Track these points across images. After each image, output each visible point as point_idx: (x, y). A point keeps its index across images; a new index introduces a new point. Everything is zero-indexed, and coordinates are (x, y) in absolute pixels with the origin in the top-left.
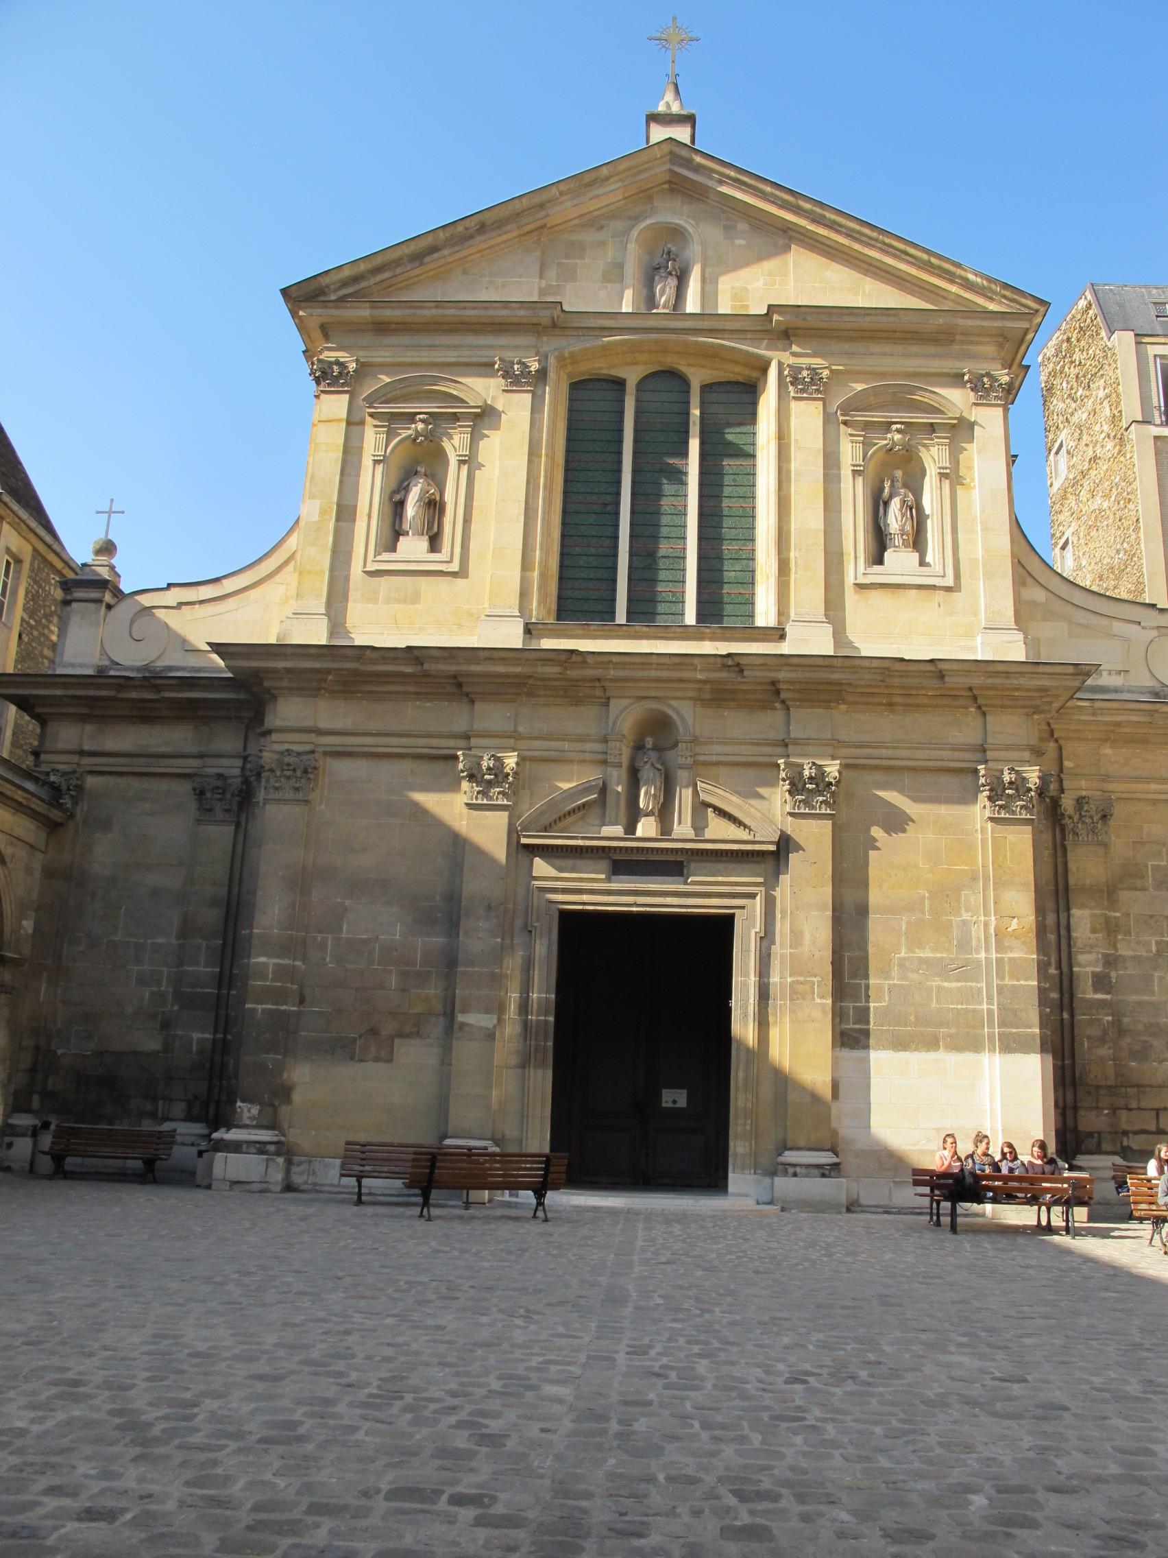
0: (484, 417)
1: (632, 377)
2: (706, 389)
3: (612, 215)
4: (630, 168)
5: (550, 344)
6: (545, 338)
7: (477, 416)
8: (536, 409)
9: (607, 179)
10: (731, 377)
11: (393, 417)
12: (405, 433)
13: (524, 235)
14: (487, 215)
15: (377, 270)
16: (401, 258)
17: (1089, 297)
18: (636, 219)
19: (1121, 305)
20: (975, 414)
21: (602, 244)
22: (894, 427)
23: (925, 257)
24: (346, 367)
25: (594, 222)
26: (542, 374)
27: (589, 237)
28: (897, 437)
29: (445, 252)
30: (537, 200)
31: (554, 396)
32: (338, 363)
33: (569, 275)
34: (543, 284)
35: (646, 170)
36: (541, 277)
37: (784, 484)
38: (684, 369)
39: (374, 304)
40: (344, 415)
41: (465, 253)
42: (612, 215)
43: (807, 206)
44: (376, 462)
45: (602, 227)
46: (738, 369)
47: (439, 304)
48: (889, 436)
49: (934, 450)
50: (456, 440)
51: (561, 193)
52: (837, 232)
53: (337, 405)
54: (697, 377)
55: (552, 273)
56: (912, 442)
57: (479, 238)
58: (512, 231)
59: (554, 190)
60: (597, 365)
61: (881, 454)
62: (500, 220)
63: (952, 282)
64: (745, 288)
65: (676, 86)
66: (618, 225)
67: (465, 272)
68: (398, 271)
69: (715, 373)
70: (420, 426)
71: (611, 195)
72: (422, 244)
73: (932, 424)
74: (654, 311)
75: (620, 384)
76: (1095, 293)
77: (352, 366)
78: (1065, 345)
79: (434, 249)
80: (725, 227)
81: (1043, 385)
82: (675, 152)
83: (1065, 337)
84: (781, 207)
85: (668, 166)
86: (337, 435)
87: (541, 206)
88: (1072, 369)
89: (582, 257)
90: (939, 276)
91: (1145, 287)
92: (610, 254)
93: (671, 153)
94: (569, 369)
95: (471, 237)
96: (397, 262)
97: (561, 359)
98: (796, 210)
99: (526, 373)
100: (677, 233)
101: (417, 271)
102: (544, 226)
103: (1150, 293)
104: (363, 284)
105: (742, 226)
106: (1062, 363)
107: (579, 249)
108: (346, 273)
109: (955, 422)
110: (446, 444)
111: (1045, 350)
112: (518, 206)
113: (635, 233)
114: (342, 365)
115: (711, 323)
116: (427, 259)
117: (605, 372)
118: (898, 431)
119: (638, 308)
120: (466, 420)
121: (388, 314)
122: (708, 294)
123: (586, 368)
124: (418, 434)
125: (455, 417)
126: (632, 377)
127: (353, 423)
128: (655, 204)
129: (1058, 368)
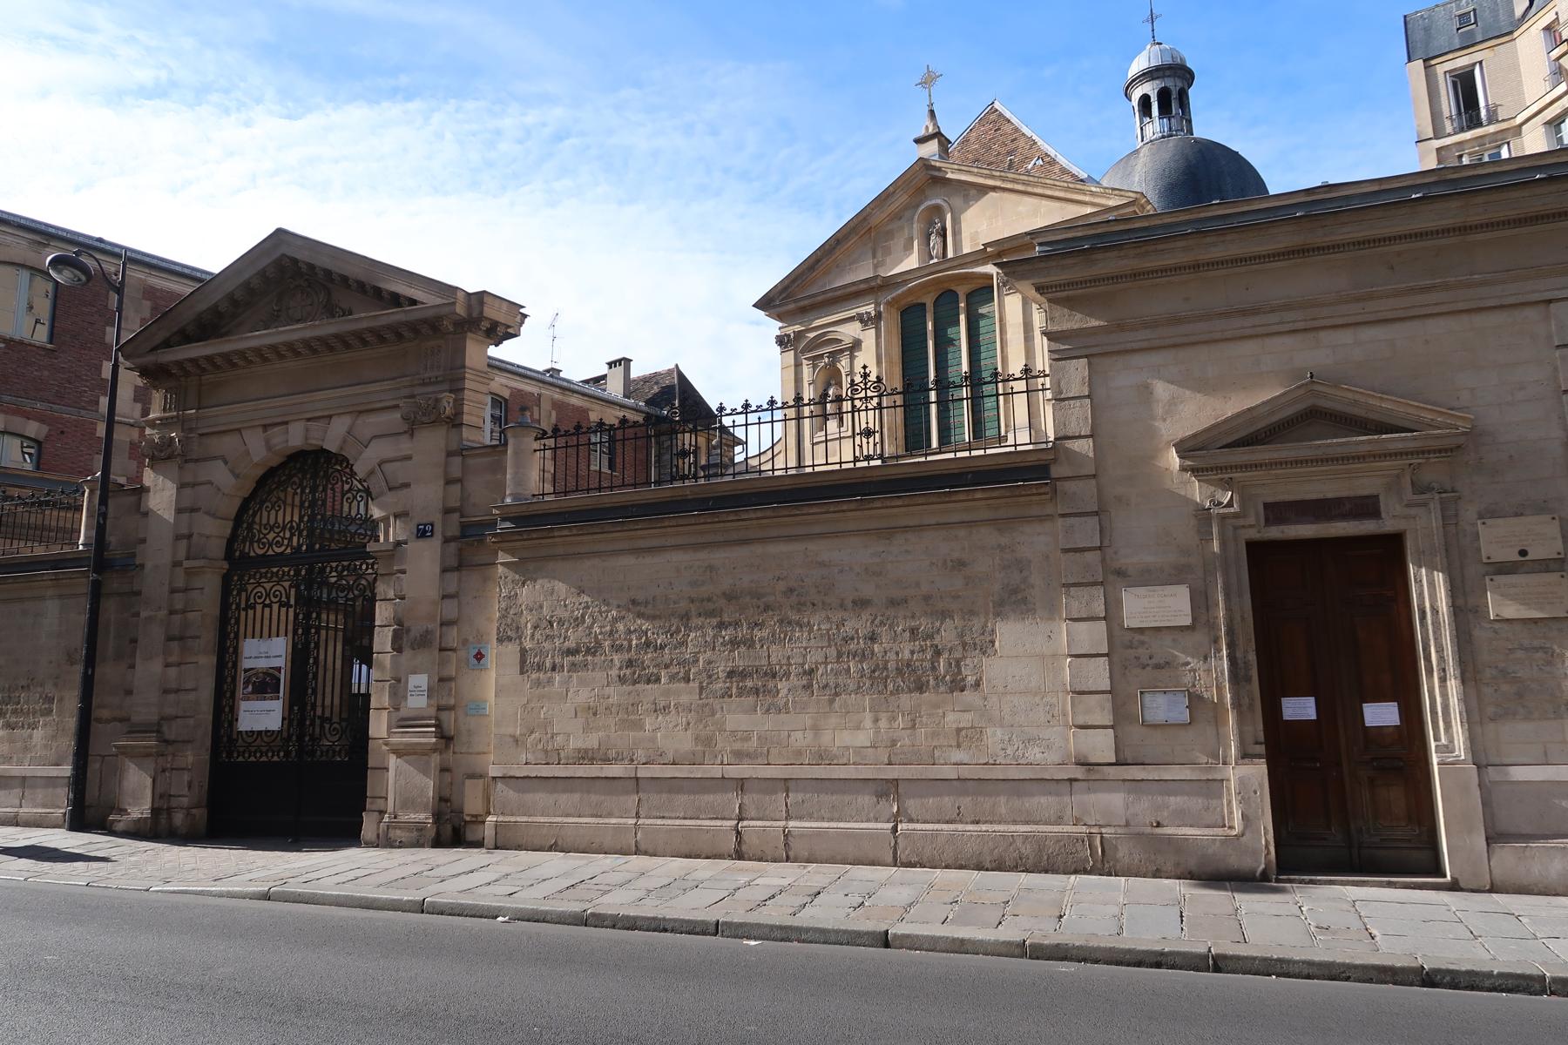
1: (929, 301)
3: (906, 207)
8: (878, 336)
10: (979, 286)
11: (814, 358)
13: (862, 236)
14: (839, 235)
15: (794, 281)
18: (918, 206)
21: (902, 228)
23: (1066, 185)
25: (897, 216)
26: (879, 316)
30: (861, 218)
31: (891, 324)
33: (888, 251)
34: (875, 261)
35: (915, 177)
36: (874, 257)
37: (1005, 348)
38: (953, 288)
39: (795, 301)
40: (793, 363)
41: (834, 257)
44: (810, 384)
45: (901, 218)
46: (981, 281)
47: (824, 293)
50: (843, 363)
51: (873, 209)
52: (1018, 183)
54: (962, 291)
55: (879, 254)
57: (839, 247)
60: (910, 299)
62: (845, 235)
63: (1085, 194)
64: (977, 232)
66: (908, 214)
67: (837, 266)
68: (804, 277)
70: (826, 360)
71: (901, 199)
72: (811, 261)
74: (931, 262)
77: (792, 335)
79: (818, 261)
84: (986, 178)
85: (924, 173)
87: (865, 219)
89: (892, 239)
90: (1077, 193)
95: (834, 248)
96: (802, 274)
97: (888, 304)
99: (870, 319)
101: (815, 274)
102: (871, 227)
104: (790, 290)
105: (973, 192)
107: (890, 235)
108: (780, 288)
110: (839, 366)
112: (852, 224)
113: (916, 217)
114: (789, 336)
116: (816, 267)
117: (915, 302)
119: (924, 262)
120: (846, 351)
121: (802, 303)
124: (826, 365)
125: (842, 351)
127: (798, 365)
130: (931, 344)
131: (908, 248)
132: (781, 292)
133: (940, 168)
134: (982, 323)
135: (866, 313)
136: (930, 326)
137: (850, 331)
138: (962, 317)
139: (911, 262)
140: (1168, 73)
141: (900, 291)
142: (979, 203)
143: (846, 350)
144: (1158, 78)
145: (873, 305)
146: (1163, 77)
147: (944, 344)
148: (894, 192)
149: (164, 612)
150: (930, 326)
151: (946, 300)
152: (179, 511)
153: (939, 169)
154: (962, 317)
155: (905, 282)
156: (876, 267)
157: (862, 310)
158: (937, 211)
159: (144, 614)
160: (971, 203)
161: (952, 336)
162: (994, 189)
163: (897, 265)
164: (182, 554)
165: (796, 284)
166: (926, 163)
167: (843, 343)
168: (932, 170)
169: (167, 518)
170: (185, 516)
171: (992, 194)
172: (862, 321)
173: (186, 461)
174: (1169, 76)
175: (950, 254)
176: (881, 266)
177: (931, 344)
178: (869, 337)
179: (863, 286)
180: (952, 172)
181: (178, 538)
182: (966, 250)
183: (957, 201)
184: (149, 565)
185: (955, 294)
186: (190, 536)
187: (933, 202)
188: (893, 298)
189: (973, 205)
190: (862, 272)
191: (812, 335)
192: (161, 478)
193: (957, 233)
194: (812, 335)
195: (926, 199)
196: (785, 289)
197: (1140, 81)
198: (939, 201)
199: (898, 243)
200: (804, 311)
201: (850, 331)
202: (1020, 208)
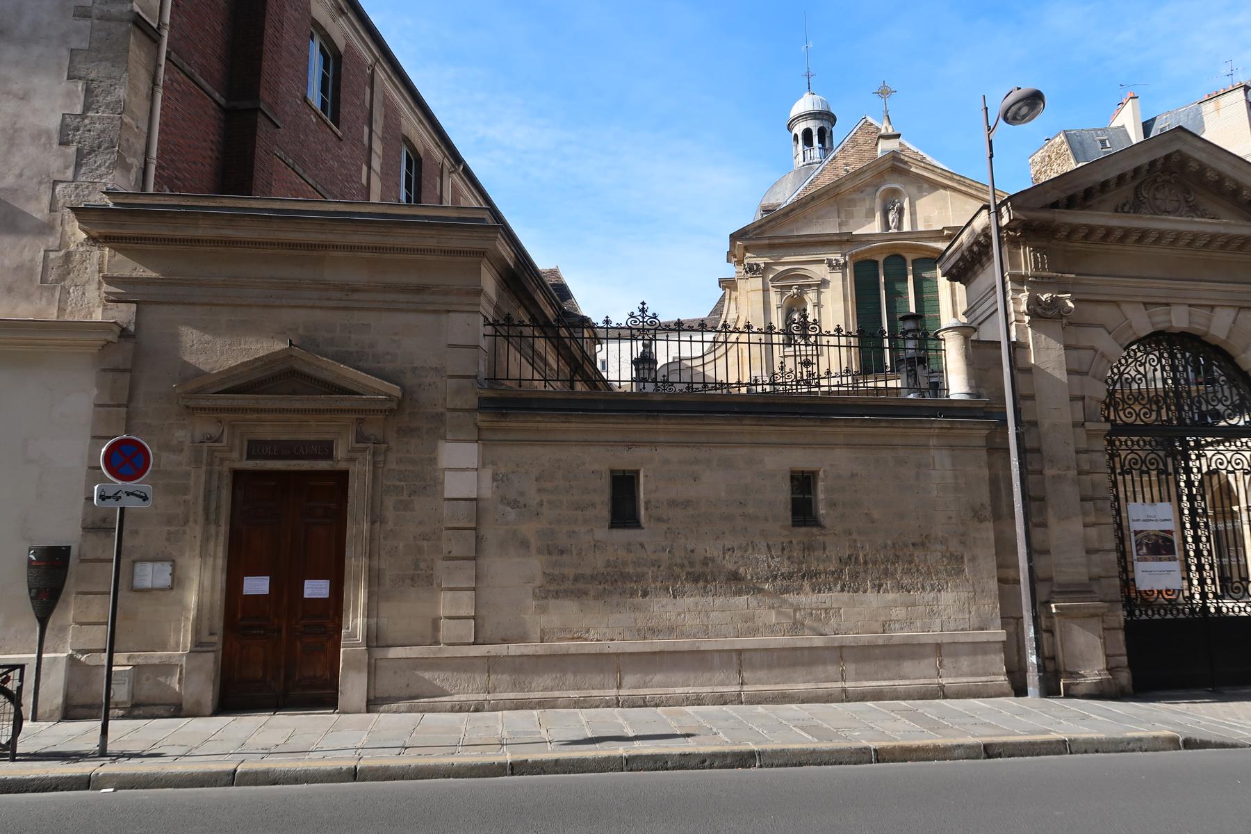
0: (823, 283)
1: (881, 259)
2: (914, 262)
3: (867, 185)
4: (876, 165)
5: (846, 249)
6: (843, 246)
7: (818, 285)
8: (844, 280)
9: (867, 170)
10: (924, 256)
11: (782, 287)
12: (789, 294)
16: (779, 216)
17: (1063, 138)
18: (877, 187)
19: (1081, 143)
21: (864, 199)
24: (759, 265)
25: (860, 190)
26: (845, 263)
27: (856, 196)
29: (798, 210)
32: (756, 264)
33: (850, 215)
38: (904, 254)
40: (761, 288)
42: (867, 185)
43: (958, 178)
44: (777, 308)
45: (862, 192)
46: (928, 253)
51: (846, 180)
52: (971, 188)
53: (757, 283)
54: (909, 258)
55: (843, 215)
58: (826, 197)
59: (844, 179)
65: (888, 116)
66: (869, 190)
67: (805, 217)
69: (916, 255)
70: (795, 291)
71: (867, 176)
74: (890, 231)
75: (876, 262)
76: (1066, 136)
77: (762, 266)
78: (1047, 159)
79: (792, 210)
80: (918, 187)
81: (1033, 176)
82: (894, 156)
83: (1047, 154)
84: (945, 178)
85: (892, 162)
86: (759, 297)
87: (838, 186)
88: (1052, 173)
91: (1094, 129)
92: (867, 204)
93: (893, 156)
94: (854, 259)
95: (809, 203)
97: (851, 257)
98: (952, 179)
99: (838, 264)
100: (895, 192)
103: (1096, 133)
104: (763, 228)
105: (926, 186)
106: (1045, 168)
107: (852, 203)
108: (757, 224)
110: (806, 297)
111: (1034, 157)
113: (878, 194)
114: (758, 265)
115: (915, 234)
119: (882, 231)
122: (913, 222)
123: (860, 258)
124: (794, 294)
125: (810, 286)
126: (881, 259)
127: (765, 290)
128: (886, 177)
129: (1043, 170)
130: (883, 292)
131: (870, 215)
132: (756, 229)
133: (907, 162)
134: (925, 284)
135: (835, 260)
136: (882, 279)
137: (819, 272)
138: (910, 278)
139: (875, 227)
140: (825, 117)
141: (863, 248)
142: (931, 195)
143: (814, 285)
144: (818, 119)
145: (840, 255)
146: (822, 119)
147: (895, 296)
148: (867, 170)
149: (1072, 473)
150: (882, 279)
151: (896, 263)
152: (1069, 372)
153: (906, 163)
154: (910, 278)
155: (869, 242)
156: (840, 225)
157: (832, 257)
158: (895, 192)
159: (1049, 472)
160: (924, 194)
161: (900, 290)
162: (946, 187)
163: (859, 228)
164: (1080, 417)
165: (770, 224)
166: (897, 155)
167: (812, 280)
168: (898, 161)
169: (1059, 377)
170: (1076, 378)
171: (942, 191)
172: (830, 265)
173: (1070, 324)
174: (825, 120)
175: (907, 227)
176: (846, 225)
177: (883, 292)
178: (836, 279)
179: (835, 238)
180: (916, 168)
182: (921, 228)
183: (913, 190)
184: (1046, 424)
185: (904, 260)
186: (1083, 398)
187: (893, 186)
188: (856, 253)
189: (926, 196)
190: (830, 227)
191: (781, 269)
192: (1043, 336)
193: (913, 214)
194: (781, 269)
195: (885, 182)
196: (760, 226)
197: (806, 118)
198: (898, 186)
199: (860, 210)
200: (772, 247)
201: (819, 272)
202: (967, 207)
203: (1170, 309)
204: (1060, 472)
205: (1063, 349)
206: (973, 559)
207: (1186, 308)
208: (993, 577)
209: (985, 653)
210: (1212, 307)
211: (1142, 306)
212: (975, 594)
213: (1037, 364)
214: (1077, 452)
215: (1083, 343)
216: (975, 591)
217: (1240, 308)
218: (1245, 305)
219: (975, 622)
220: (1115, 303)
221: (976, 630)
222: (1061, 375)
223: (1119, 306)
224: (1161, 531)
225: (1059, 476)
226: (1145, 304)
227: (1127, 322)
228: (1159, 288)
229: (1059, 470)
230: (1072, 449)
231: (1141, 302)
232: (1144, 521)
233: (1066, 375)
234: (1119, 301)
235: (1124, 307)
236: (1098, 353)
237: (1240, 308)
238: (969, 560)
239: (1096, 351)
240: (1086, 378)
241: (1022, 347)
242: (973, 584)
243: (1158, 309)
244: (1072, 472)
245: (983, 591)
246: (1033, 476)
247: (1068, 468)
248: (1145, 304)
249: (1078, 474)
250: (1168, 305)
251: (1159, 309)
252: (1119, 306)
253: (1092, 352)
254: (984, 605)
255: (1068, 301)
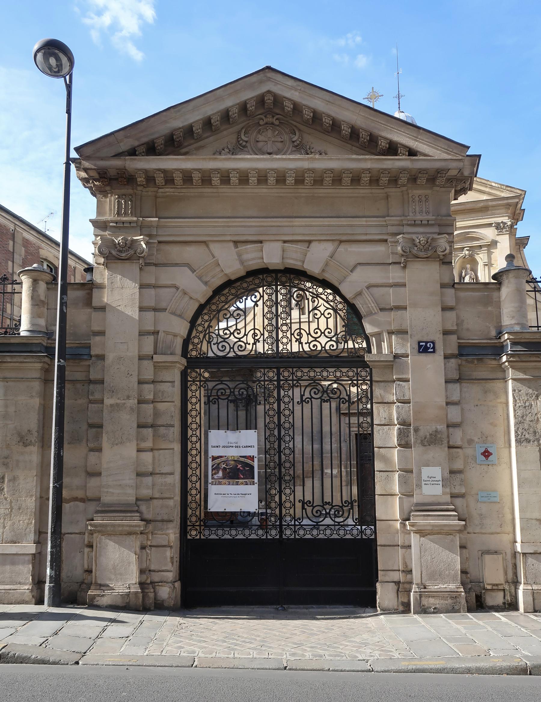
20: (498, 238)
22: (465, 249)
28: (467, 252)
48: (464, 252)
49: (481, 255)
56: (473, 254)
61: (461, 260)
73: (480, 246)
109: (490, 243)
118: (467, 250)
149: (133, 402)
152: (142, 309)
159: (108, 401)
164: (149, 349)
169: (130, 314)
170: (150, 315)
173: (147, 264)
181: (142, 333)
184: (110, 357)
186: (156, 333)
192: (119, 277)
203: (262, 247)
204: (119, 401)
205: (138, 287)
206: (14, 479)
207: (279, 245)
208: (32, 496)
209: (13, 563)
210: (310, 242)
211: (232, 244)
212: (11, 511)
213: (108, 302)
214: (140, 382)
215: (164, 281)
216: (12, 508)
217: (341, 242)
218: (344, 238)
219: (8, 535)
220: (204, 242)
221: (8, 543)
222: (133, 312)
223: (207, 246)
224: (240, 457)
225: (118, 405)
226: (236, 243)
227: (215, 259)
228: (251, 227)
229: (118, 399)
230: (135, 379)
231: (230, 241)
232: (224, 447)
233: (138, 311)
234: (208, 241)
235: (212, 246)
236: (180, 290)
237: (341, 242)
238: (9, 481)
239: (177, 288)
240: (161, 315)
241: (97, 288)
242: (11, 502)
243: (248, 246)
244: (130, 401)
245: (19, 509)
246: (93, 405)
247: (128, 397)
248: (236, 243)
249: (138, 403)
250: (261, 242)
251: (249, 246)
252: (207, 246)
253: (174, 290)
254: (19, 521)
255: (142, 243)
